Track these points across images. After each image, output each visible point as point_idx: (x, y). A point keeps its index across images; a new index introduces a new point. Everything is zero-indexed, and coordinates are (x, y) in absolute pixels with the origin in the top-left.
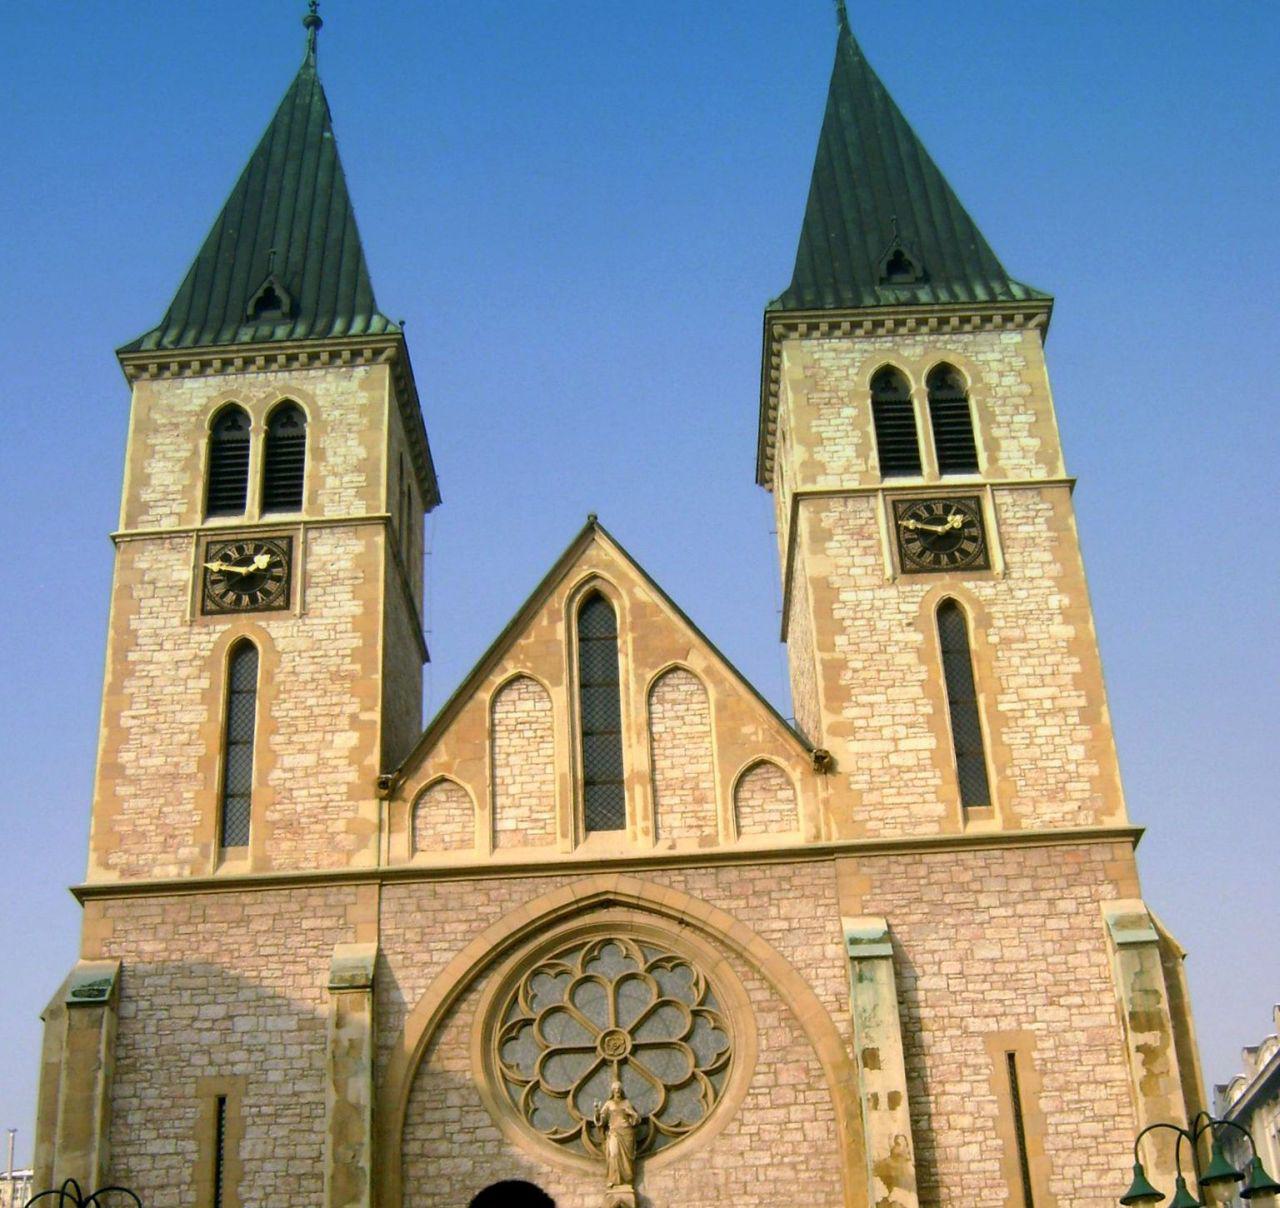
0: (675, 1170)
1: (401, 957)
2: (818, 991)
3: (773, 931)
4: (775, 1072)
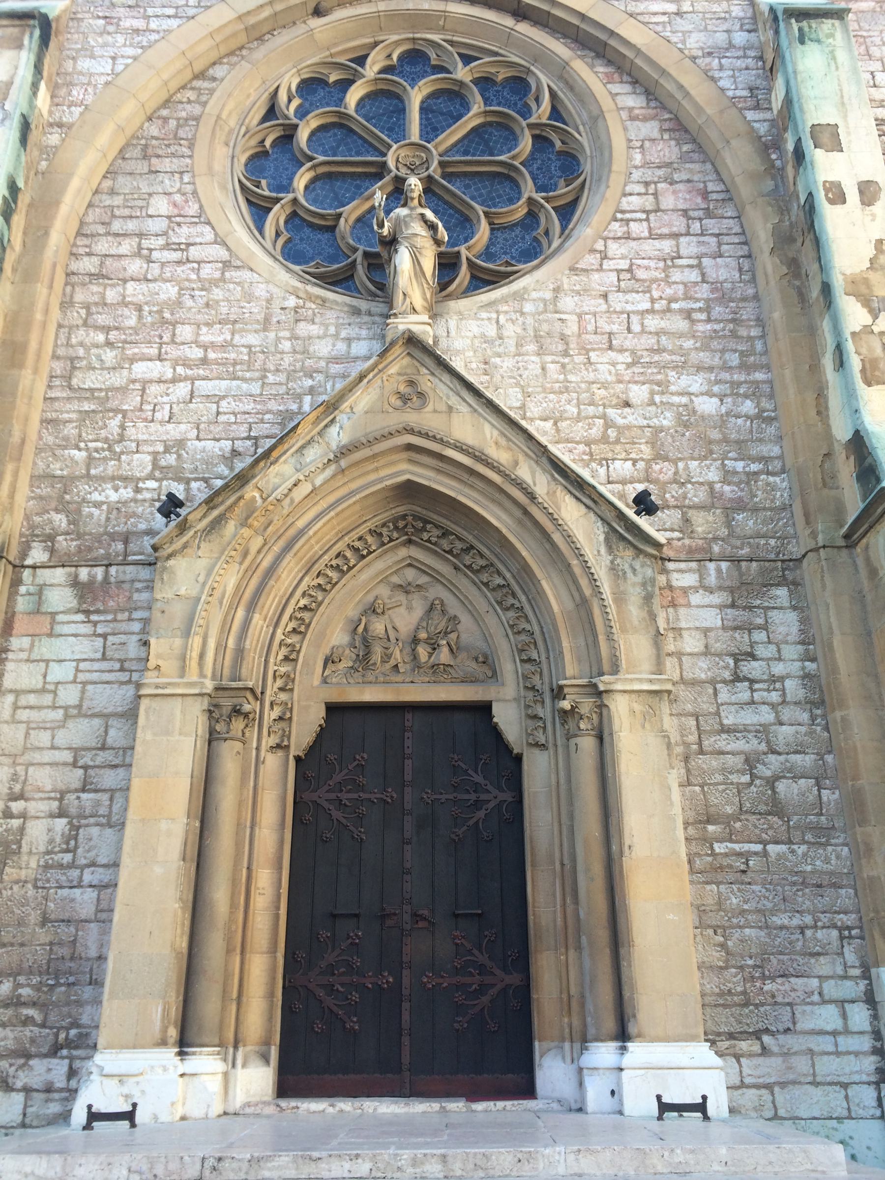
0: (497, 312)
1: (102, 22)
2: (724, 83)
3: (655, 14)
4: (655, 194)
